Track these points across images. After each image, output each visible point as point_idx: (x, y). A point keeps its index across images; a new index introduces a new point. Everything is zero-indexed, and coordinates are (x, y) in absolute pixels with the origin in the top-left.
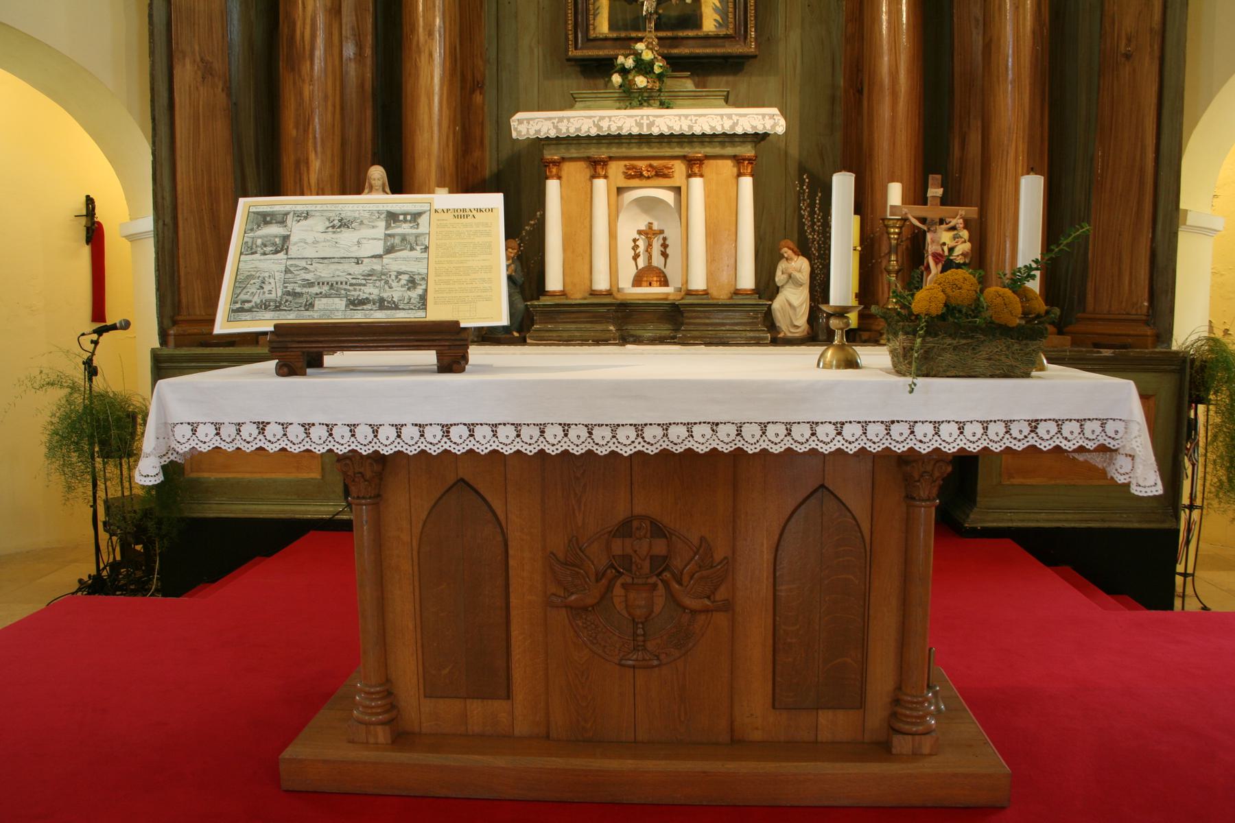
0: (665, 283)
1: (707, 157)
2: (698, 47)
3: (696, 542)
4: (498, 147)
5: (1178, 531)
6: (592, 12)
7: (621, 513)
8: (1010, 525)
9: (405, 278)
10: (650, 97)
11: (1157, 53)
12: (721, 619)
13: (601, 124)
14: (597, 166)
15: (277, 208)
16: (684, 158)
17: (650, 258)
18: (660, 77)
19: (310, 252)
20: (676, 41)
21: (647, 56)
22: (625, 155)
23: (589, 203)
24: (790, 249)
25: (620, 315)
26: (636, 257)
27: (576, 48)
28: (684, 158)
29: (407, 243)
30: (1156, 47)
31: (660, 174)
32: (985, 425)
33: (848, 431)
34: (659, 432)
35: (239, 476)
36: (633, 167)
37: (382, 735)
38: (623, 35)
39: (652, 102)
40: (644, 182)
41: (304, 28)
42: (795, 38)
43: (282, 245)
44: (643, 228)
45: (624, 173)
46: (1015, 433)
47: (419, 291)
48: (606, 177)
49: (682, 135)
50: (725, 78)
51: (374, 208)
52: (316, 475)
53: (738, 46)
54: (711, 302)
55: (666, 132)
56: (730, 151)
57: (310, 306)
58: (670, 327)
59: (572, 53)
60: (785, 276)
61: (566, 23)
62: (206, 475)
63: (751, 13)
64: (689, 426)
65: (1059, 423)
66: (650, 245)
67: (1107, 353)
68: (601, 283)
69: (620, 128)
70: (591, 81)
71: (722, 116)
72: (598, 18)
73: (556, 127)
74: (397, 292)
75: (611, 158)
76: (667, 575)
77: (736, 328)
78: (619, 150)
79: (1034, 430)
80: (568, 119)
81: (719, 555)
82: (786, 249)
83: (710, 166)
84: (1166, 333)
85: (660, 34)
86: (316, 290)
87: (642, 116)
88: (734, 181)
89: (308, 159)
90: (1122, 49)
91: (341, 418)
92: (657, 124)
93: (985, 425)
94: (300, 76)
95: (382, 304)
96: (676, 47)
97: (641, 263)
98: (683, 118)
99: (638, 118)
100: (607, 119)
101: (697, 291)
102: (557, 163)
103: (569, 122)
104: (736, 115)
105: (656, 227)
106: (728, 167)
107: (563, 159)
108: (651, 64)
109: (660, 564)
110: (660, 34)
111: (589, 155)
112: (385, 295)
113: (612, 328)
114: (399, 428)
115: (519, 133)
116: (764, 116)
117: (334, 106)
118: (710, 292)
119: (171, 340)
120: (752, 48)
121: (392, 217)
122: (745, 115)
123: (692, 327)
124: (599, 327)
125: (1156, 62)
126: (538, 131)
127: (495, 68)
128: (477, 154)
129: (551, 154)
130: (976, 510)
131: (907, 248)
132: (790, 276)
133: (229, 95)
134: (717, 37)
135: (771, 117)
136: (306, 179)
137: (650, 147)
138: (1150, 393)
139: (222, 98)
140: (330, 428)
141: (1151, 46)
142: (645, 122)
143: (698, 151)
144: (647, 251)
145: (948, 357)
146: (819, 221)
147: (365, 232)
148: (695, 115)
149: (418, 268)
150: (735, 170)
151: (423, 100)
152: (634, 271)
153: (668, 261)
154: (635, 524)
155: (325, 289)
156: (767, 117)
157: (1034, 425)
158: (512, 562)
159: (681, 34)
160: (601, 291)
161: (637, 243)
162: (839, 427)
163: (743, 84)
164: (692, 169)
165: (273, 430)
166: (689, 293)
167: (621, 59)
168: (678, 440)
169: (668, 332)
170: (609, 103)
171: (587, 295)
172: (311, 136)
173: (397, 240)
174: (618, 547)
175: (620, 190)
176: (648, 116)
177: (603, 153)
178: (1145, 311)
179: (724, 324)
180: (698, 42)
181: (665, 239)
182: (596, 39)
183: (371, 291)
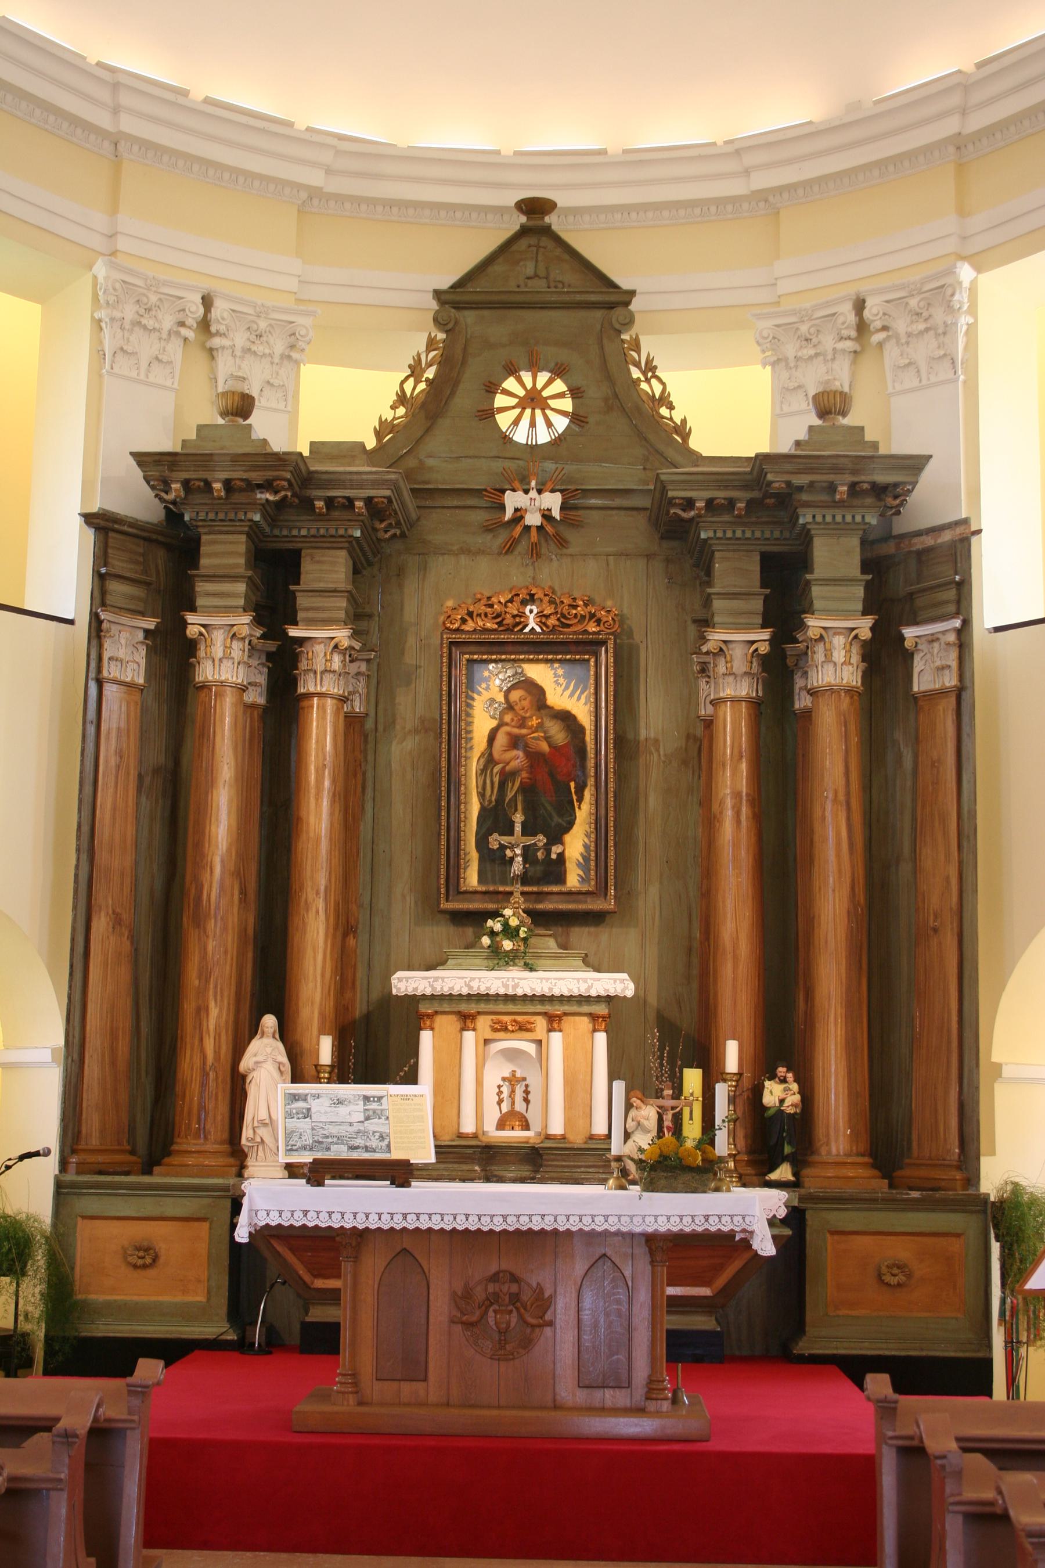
0: (526, 1127)
1: (565, 1014)
2: (562, 902)
3: (534, 1285)
4: (368, 989)
5: (988, 1363)
6: (463, 866)
7: (494, 1268)
8: (835, 1352)
9: (378, 1134)
10: (515, 957)
11: (955, 930)
12: (548, 1331)
13: (472, 984)
14: (467, 1020)
15: (300, 1091)
16: (545, 1014)
17: (513, 1103)
18: (525, 940)
19: (323, 1119)
20: (540, 896)
21: (514, 922)
22: (492, 1010)
23: (458, 1053)
24: (639, 1099)
25: (484, 1156)
26: (500, 1102)
27: (447, 901)
28: (545, 1014)
29: (377, 1114)
30: (955, 925)
31: (523, 1028)
32: (681, 1217)
33: (611, 1220)
34: (515, 1219)
35: (127, 1298)
36: (499, 1022)
37: (352, 1399)
38: (491, 889)
39: (517, 961)
40: (509, 1035)
41: (211, 890)
42: (654, 891)
43: (307, 1114)
44: (507, 1075)
45: (491, 1026)
46: (697, 1222)
47: (386, 1142)
48: (474, 1029)
49: (543, 996)
50: (586, 930)
51: (355, 1093)
52: (201, 1298)
53: (599, 902)
54: (567, 1145)
55: (529, 993)
56: (586, 1009)
57: (328, 1149)
58: (530, 1168)
59: (445, 905)
60: (635, 1123)
61: (439, 877)
62: (92, 1297)
63: (611, 872)
64: (530, 1216)
65: (720, 1217)
66: (513, 1091)
67: (915, 1194)
68: (468, 1127)
69: (488, 988)
70: (460, 929)
71: (578, 980)
72: (469, 871)
73: (431, 986)
74: (374, 1143)
75: (479, 1013)
76: (518, 1304)
77: (590, 1170)
78: (488, 1006)
79: (707, 1220)
80: (443, 979)
81: (547, 1295)
82: (634, 1099)
83: (568, 1022)
84: (973, 1178)
85: (526, 889)
86: (330, 1140)
87: (508, 978)
88: (590, 1035)
89: (208, 1007)
90: (931, 924)
91: (349, 1210)
92: (521, 986)
93: (681, 1217)
94: (205, 932)
95: (367, 1149)
96: (541, 902)
97: (505, 1107)
98: (544, 981)
99: (505, 980)
100: (477, 980)
101: (555, 1135)
102: (430, 1016)
103: (443, 981)
104: (591, 979)
105: (518, 1075)
106: (584, 1023)
107: (436, 1013)
108: (517, 929)
109: (515, 1298)
110: (526, 889)
111: (460, 1009)
112: (368, 1144)
113: (477, 1168)
114: (380, 1215)
115: (398, 989)
116: (615, 980)
117: (232, 959)
118: (567, 1136)
119: (72, 1168)
120: (611, 905)
121: (366, 1099)
122: (599, 980)
123: (548, 1169)
124: (465, 1167)
125: (956, 937)
126: (416, 989)
127: (369, 913)
128: (348, 995)
129: (425, 1008)
130: (805, 1338)
131: (748, 1096)
132: (639, 1124)
133: (132, 943)
134: (579, 893)
135: (622, 981)
136: (205, 1024)
137: (515, 1004)
138: (959, 1231)
139: (127, 946)
140: (343, 1214)
141: (952, 923)
142: (511, 983)
143: (558, 1009)
144: (510, 1097)
145: (663, 1182)
146: (666, 1072)
147: (352, 1107)
148: (555, 979)
149: (382, 1129)
150: (591, 1026)
151: (309, 952)
152: (498, 1115)
153: (529, 1106)
154: (501, 1275)
155: (335, 1140)
156: (618, 981)
157: (707, 1218)
158: (431, 1298)
159: (545, 889)
160: (468, 1134)
161: (502, 1089)
162: (606, 1218)
163: (604, 937)
164: (552, 1024)
165: (312, 1215)
166: (548, 1137)
167: (490, 923)
168: (524, 1224)
169: (528, 1173)
170: (478, 961)
171: (454, 1137)
172: (212, 986)
173: (371, 1113)
174: (491, 1288)
175: (487, 1042)
176: (513, 978)
177: (472, 1008)
178: (956, 1157)
179: (579, 1167)
180: (562, 897)
181: (527, 1086)
182: (466, 892)
183: (359, 1142)
